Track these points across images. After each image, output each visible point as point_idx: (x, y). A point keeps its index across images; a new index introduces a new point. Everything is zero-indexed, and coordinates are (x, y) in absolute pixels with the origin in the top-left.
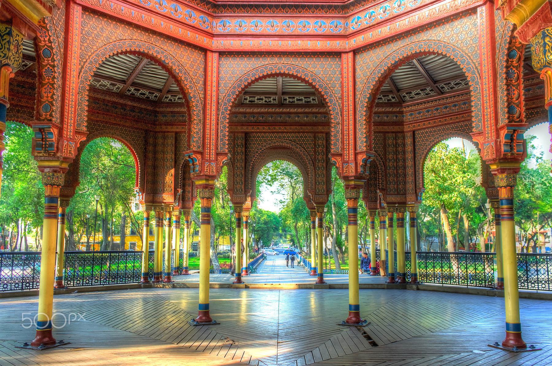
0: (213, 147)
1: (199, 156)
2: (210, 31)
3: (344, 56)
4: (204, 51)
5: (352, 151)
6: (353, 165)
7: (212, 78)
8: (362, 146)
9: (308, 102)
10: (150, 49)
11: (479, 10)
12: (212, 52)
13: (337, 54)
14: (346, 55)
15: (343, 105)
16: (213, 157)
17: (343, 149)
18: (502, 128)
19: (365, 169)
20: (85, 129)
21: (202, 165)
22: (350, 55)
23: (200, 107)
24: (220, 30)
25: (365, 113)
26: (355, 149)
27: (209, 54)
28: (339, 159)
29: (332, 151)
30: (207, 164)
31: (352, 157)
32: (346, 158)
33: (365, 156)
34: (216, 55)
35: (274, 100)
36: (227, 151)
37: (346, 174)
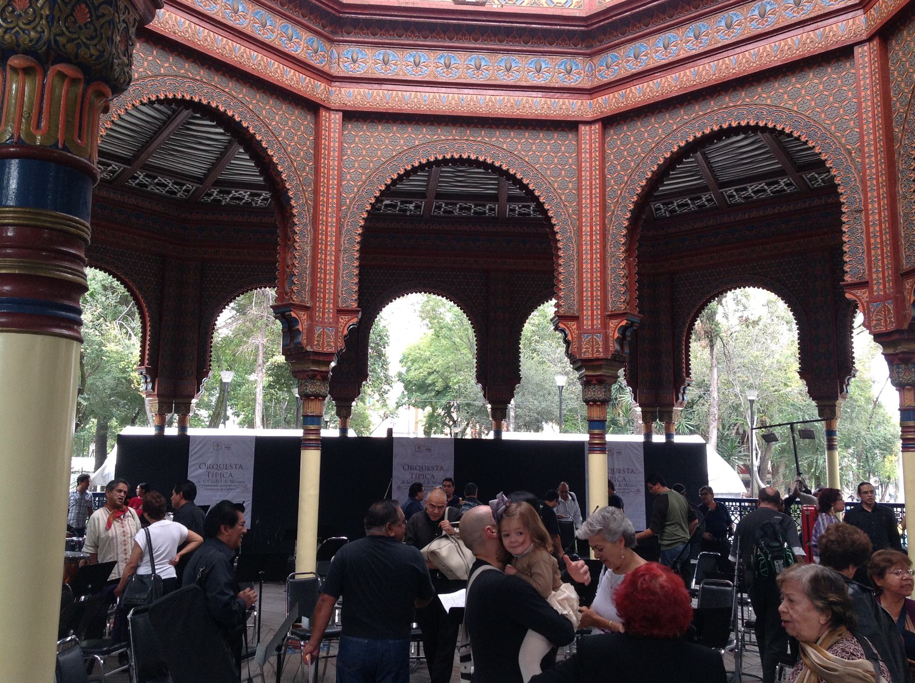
0: (330, 296)
1: (303, 316)
2: (326, 69)
3: (583, 129)
4: (312, 107)
5: (598, 312)
6: (599, 338)
7: (331, 161)
8: (618, 301)
9: (524, 214)
10: (212, 97)
11: (858, 50)
12: (328, 109)
13: (569, 126)
14: (587, 128)
15: (581, 222)
16: (330, 316)
17: (581, 309)
19: (622, 346)
21: (311, 330)
22: (597, 127)
23: (307, 220)
24: (344, 68)
25: (623, 240)
26: (604, 307)
27: (324, 113)
30: (318, 330)
31: (598, 323)
32: (587, 324)
33: (624, 323)
34: (337, 117)
35: (491, 209)
36: (355, 305)
37: (589, 356)
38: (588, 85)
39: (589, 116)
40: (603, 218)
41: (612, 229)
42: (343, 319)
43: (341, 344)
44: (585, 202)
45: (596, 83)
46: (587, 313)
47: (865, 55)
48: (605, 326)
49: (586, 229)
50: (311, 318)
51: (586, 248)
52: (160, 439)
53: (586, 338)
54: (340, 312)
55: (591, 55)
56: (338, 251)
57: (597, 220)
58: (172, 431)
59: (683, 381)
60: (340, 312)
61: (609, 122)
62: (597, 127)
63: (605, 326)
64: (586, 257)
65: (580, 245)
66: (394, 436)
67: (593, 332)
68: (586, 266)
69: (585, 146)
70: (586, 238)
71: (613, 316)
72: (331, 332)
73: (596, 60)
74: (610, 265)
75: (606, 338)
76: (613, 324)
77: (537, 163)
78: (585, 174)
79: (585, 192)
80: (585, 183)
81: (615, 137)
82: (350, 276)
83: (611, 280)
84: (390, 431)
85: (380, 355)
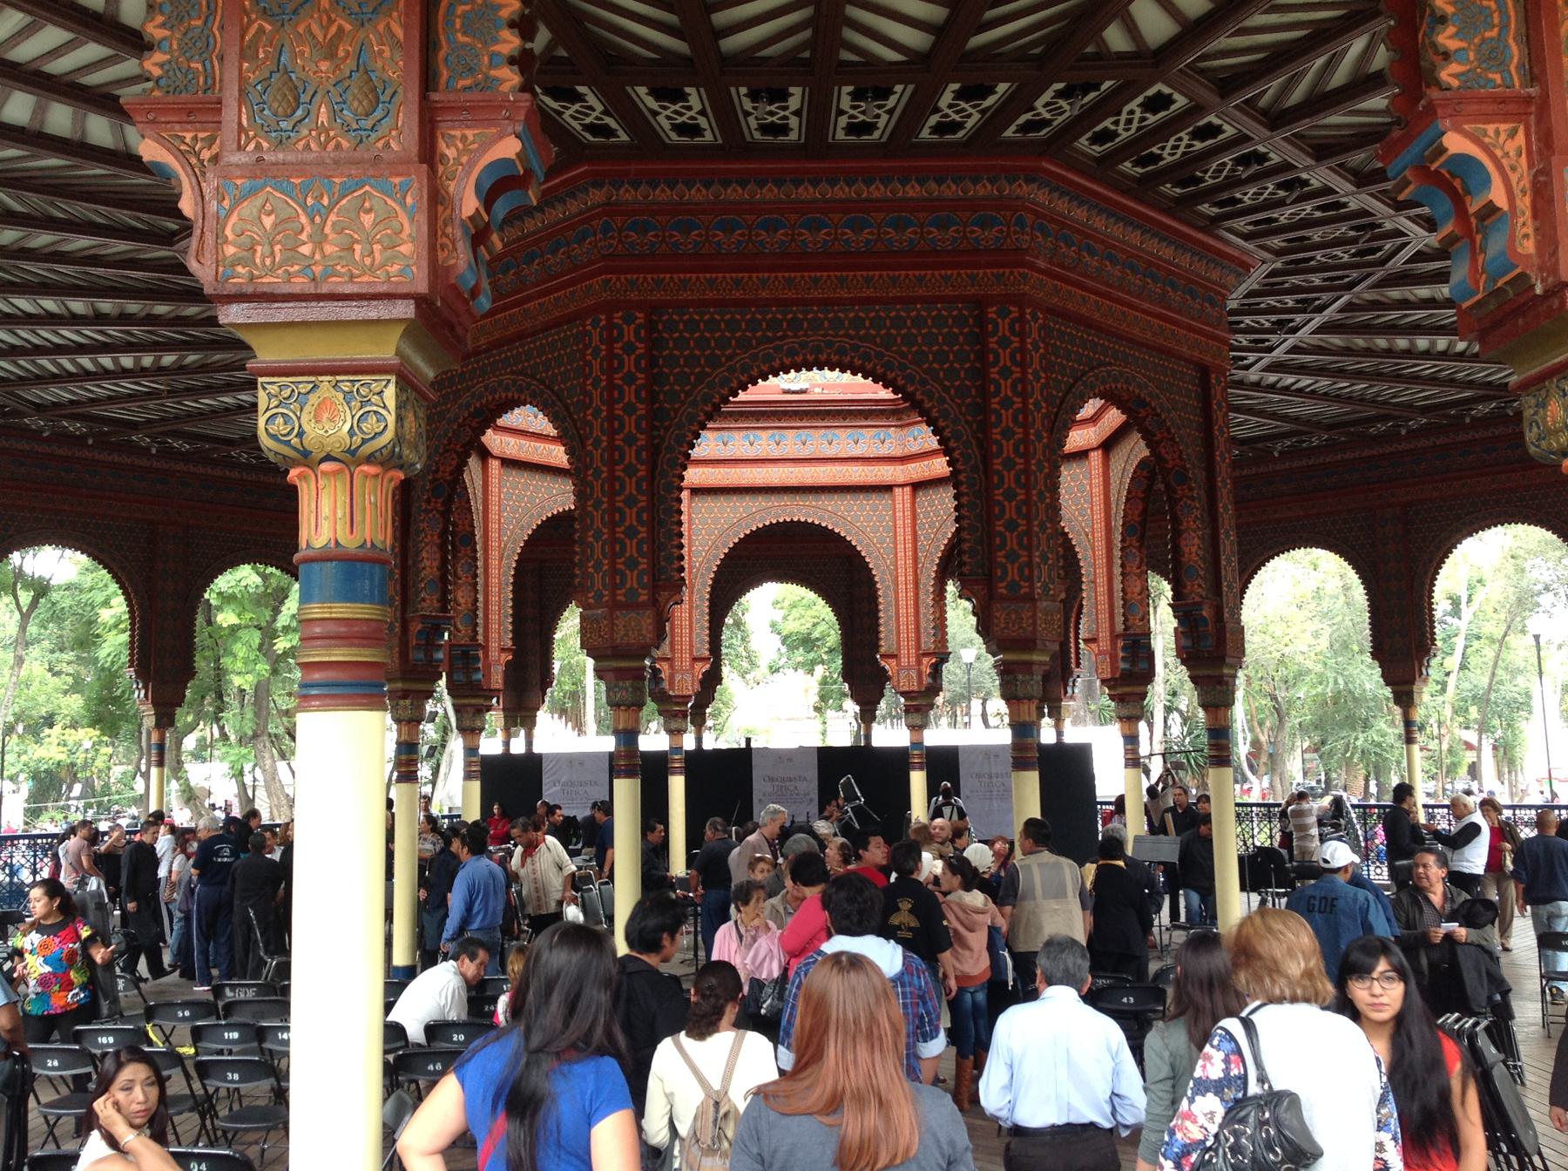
1: (665, 666)
3: (898, 491)
6: (914, 674)
13: (887, 488)
17: (899, 648)
18: (1118, 636)
20: (509, 643)
21: (672, 677)
22: (908, 489)
26: (918, 647)
28: (893, 662)
29: (882, 650)
30: (678, 677)
32: (904, 662)
36: (707, 653)
37: (906, 689)
38: (899, 453)
39: (901, 480)
40: (915, 571)
41: (923, 580)
42: (698, 665)
43: (697, 687)
44: (900, 555)
45: (906, 452)
46: (904, 652)
47: (1096, 456)
48: (919, 662)
49: (901, 579)
50: (672, 667)
51: (902, 595)
52: (507, 756)
53: (903, 674)
54: (695, 659)
55: (901, 426)
56: (691, 608)
57: (910, 570)
58: (518, 747)
59: (1071, 673)
60: (695, 659)
61: (917, 486)
62: (908, 489)
63: (919, 662)
64: (902, 603)
65: (897, 593)
66: (753, 745)
67: (909, 668)
68: (902, 611)
69: (899, 506)
70: (902, 587)
71: (925, 655)
72: (688, 677)
73: (906, 430)
74: (922, 610)
75: (920, 674)
76: (925, 660)
77: (856, 522)
78: (900, 531)
79: (900, 547)
80: (900, 538)
81: (922, 497)
82: (702, 628)
83: (923, 625)
84: (748, 740)
85: (738, 624)
